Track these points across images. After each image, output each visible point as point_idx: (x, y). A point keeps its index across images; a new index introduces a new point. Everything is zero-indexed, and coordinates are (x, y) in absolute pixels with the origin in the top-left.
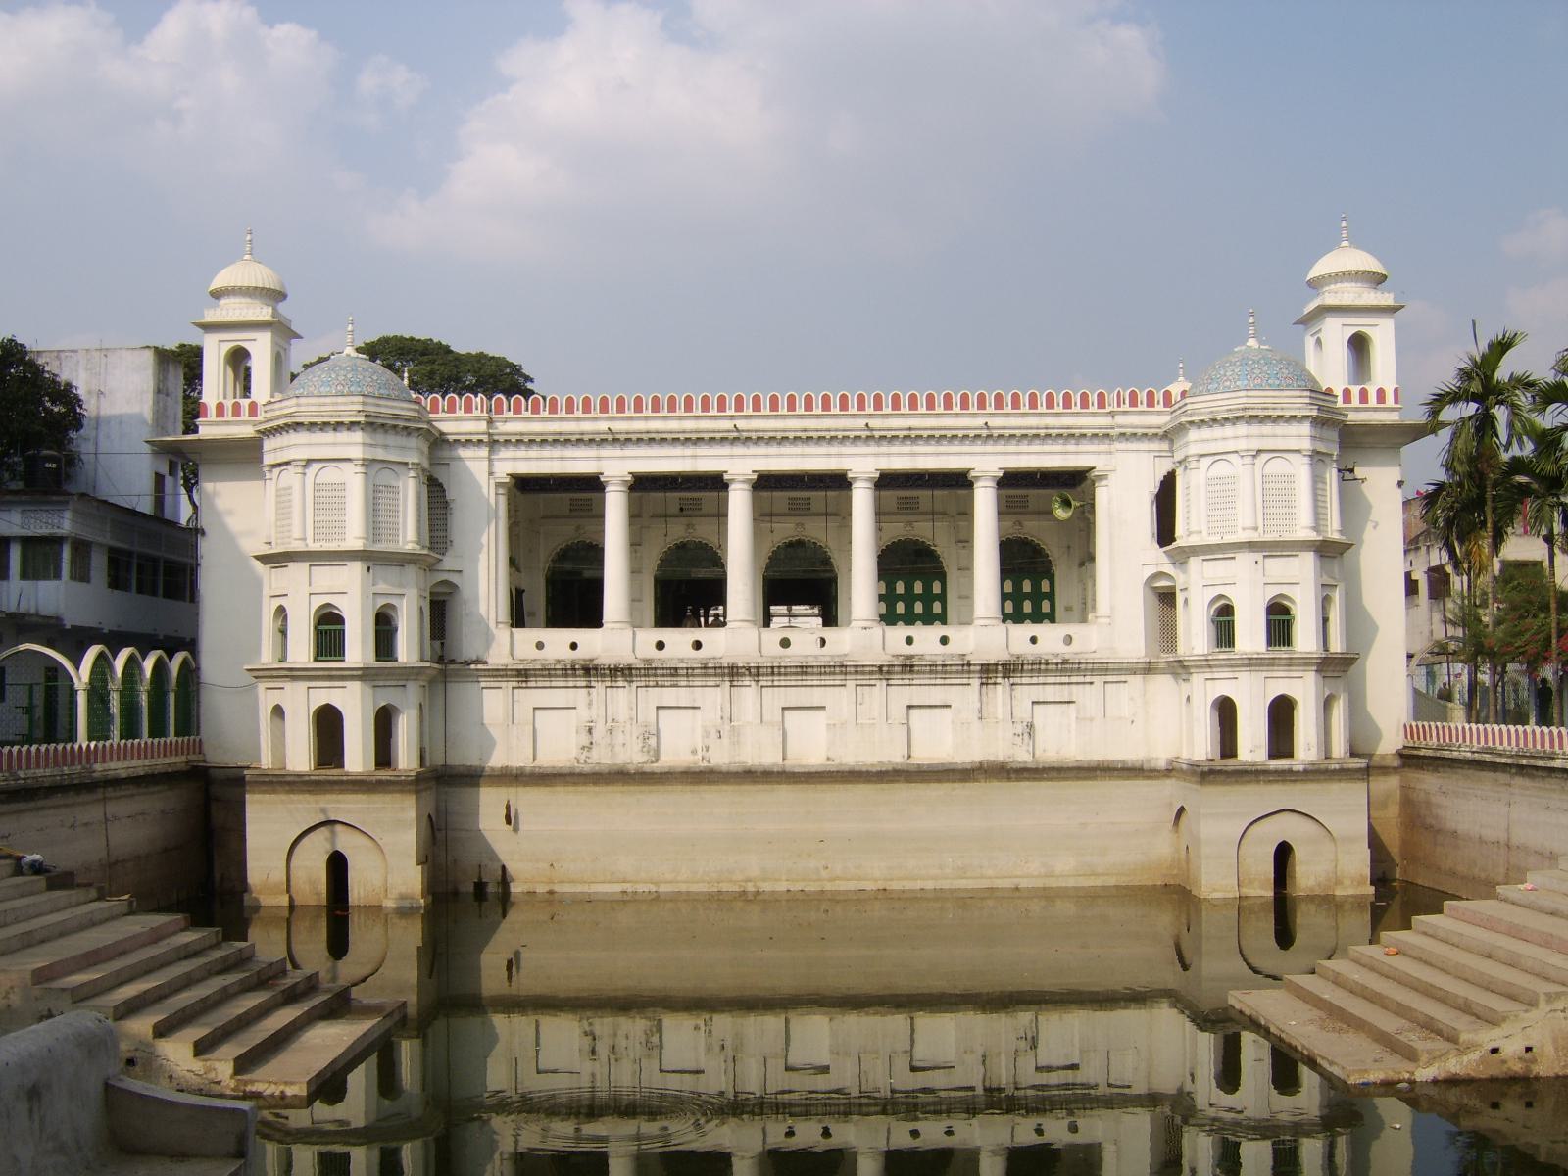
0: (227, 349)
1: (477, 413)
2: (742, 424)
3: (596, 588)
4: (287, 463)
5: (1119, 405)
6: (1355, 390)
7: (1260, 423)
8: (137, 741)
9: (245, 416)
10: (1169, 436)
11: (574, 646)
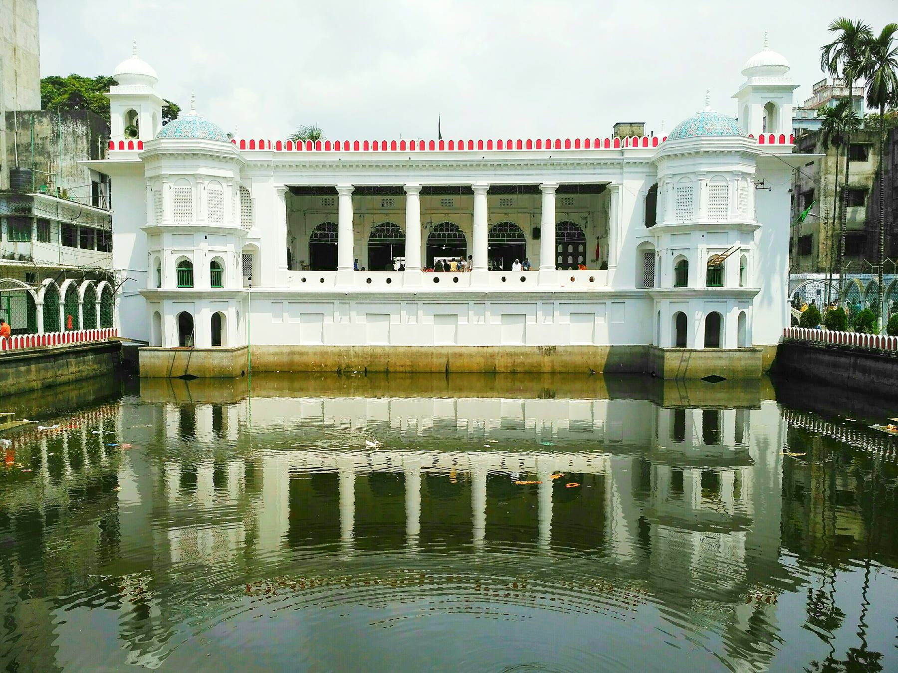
3: (335, 249)
4: (158, 176)
6: (767, 136)
11: (322, 280)
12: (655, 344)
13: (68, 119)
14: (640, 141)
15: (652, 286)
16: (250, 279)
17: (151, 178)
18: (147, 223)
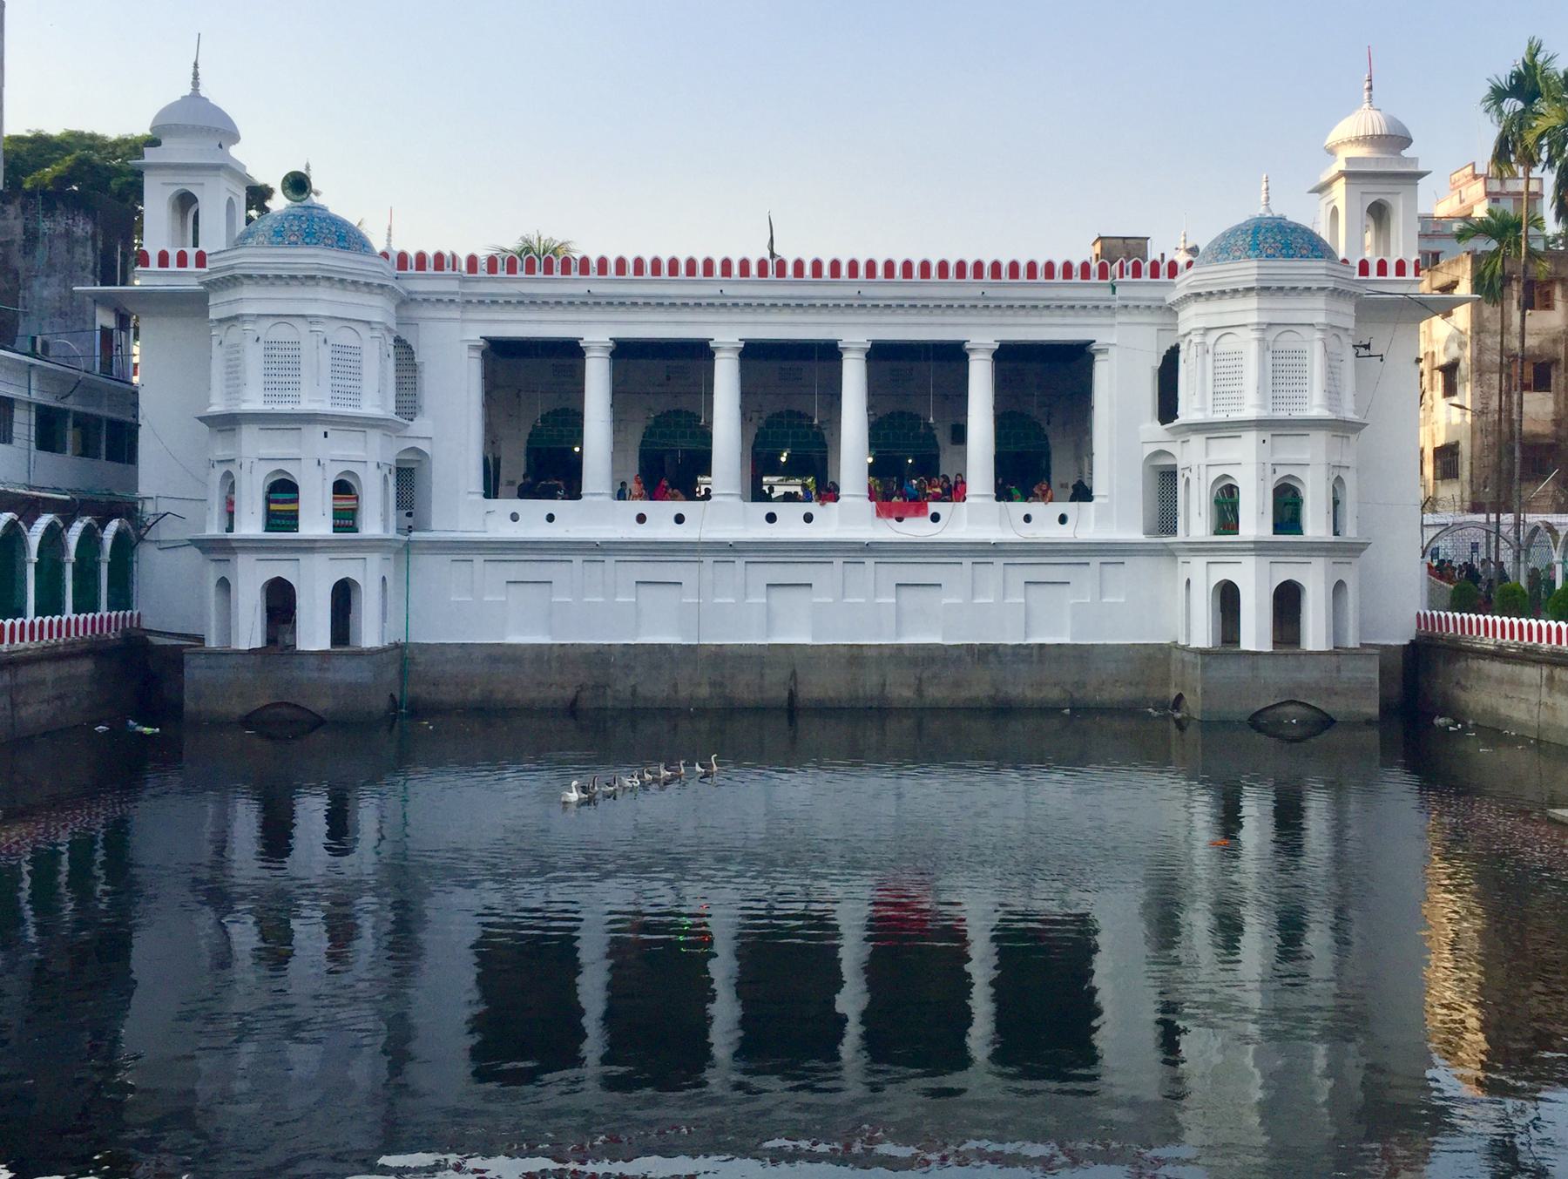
0: (171, 193)
1: (448, 271)
2: (729, 290)
4: (236, 318)
5: (1121, 276)
7: (1271, 295)
8: (57, 618)
9: (191, 267)
10: (1171, 310)
11: (551, 518)
12: (1182, 642)
13: (57, 209)
14: (1146, 266)
15: (1173, 531)
16: (409, 515)
17: (220, 321)
18: (210, 405)
